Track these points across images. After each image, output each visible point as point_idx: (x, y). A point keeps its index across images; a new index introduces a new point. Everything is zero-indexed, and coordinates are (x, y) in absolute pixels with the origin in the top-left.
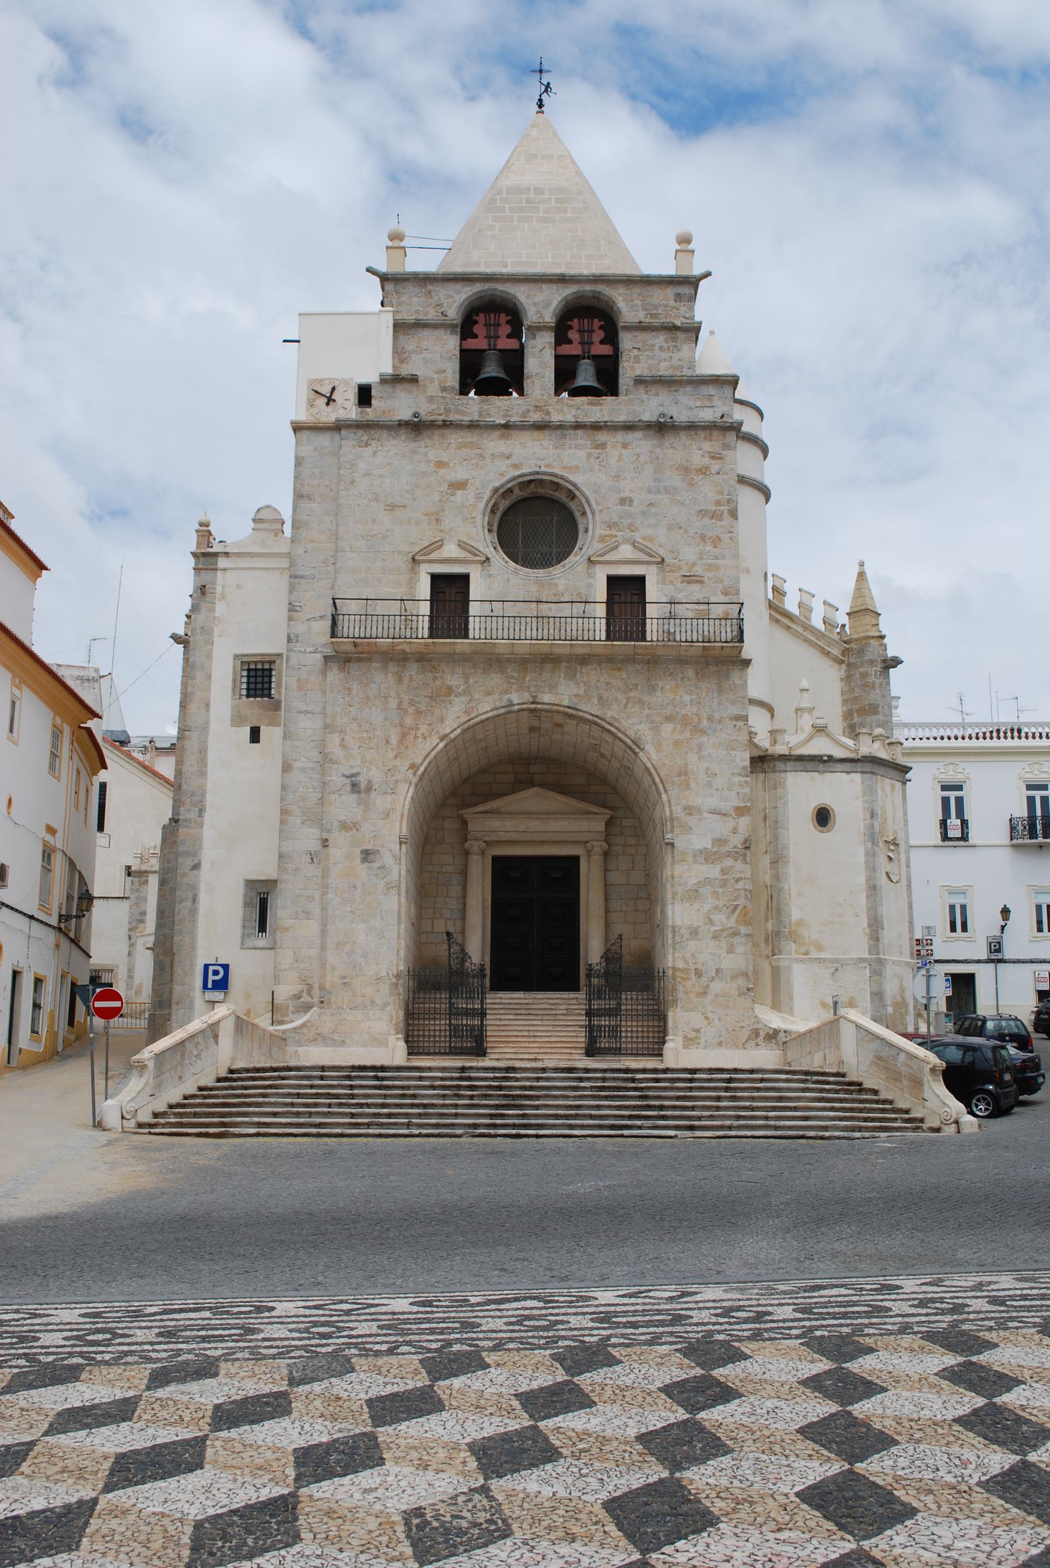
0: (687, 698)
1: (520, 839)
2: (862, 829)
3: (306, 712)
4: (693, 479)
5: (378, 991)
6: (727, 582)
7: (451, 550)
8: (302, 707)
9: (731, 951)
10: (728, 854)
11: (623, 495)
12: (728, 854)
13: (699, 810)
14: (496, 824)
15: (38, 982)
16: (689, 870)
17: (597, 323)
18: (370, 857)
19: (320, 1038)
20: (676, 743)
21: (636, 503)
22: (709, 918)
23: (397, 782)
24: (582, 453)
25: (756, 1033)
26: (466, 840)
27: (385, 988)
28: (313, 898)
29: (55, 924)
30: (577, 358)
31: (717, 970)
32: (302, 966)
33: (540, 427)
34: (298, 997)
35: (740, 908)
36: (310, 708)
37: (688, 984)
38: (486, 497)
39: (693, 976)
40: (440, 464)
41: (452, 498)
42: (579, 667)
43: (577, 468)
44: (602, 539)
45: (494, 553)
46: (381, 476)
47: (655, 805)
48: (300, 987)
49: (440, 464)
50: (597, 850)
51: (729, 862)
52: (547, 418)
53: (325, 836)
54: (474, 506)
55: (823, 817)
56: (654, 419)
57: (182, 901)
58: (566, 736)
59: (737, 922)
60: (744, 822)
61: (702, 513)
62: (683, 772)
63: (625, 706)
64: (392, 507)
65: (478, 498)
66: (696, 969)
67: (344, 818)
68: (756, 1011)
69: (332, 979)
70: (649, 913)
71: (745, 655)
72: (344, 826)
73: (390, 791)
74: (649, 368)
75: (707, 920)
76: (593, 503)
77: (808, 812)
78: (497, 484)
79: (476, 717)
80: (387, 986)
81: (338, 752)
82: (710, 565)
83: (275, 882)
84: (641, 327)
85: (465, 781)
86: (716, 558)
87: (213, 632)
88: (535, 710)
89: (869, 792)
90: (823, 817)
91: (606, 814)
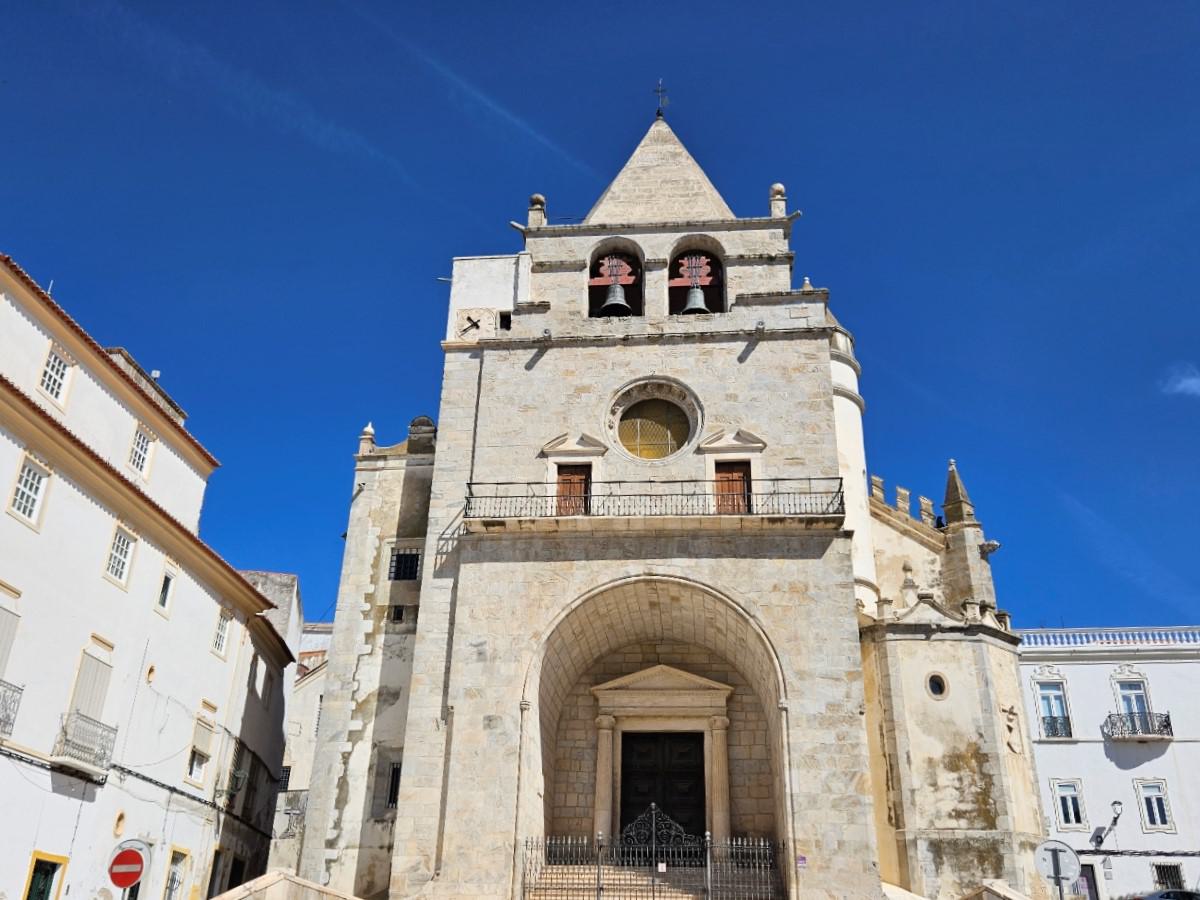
1: (646, 714)
2: (978, 697)
4: (791, 377)
5: (494, 862)
6: (828, 463)
7: (572, 444)
9: (852, 821)
10: (844, 720)
11: (728, 392)
12: (844, 720)
13: (811, 675)
14: (623, 699)
15: (177, 858)
16: (804, 735)
17: (704, 260)
18: (493, 723)
21: (740, 398)
22: (827, 786)
23: (521, 649)
24: (691, 360)
26: (597, 715)
27: (501, 858)
28: (437, 765)
29: (209, 799)
31: (841, 844)
32: (421, 835)
33: (652, 340)
34: (415, 869)
35: (859, 775)
39: (814, 848)
40: (569, 373)
41: (578, 400)
42: (690, 541)
43: (687, 370)
44: (711, 429)
45: (615, 444)
46: (516, 384)
49: (569, 373)
50: (719, 724)
51: (845, 728)
54: (597, 405)
55: (937, 685)
58: (684, 612)
59: (856, 789)
62: (794, 638)
63: (735, 576)
64: (526, 409)
65: (600, 398)
66: (817, 841)
67: (469, 685)
70: (771, 786)
71: (847, 526)
73: (513, 659)
75: (825, 788)
76: (701, 399)
78: (617, 387)
79: (596, 588)
80: (503, 858)
84: (742, 260)
85: (597, 661)
86: (816, 442)
87: (368, 522)
88: (651, 581)
89: (980, 662)
90: (937, 685)
91: (726, 690)
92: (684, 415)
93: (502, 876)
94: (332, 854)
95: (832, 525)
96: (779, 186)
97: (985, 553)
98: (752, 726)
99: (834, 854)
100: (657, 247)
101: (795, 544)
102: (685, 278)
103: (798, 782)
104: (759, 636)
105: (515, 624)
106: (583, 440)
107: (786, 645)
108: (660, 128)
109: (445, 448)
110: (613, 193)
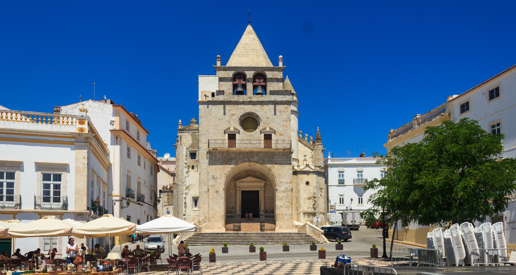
0: (280, 160)
3: (203, 163)
6: (289, 135)
7: (232, 129)
8: (203, 162)
9: (288, 210)
13: (282, 182)
19: (208, 228)
20: (278, 169)
21: (270, 118)
24: (259, 108)
25: (293, 226)
30: (258, 86)
31: (286, 214)
34: (204, 220)
36: (204, 162)
37: (280, 216)
38: (239, 117)
43: (258, 111)
44: (263, 126)
46: (217, 113)
47: (274, 181)
48: (204, 218)
51: (288, 193)
52: (251, 100)
53: (208, 188)
55: (307, 183)
56: (273, 100)
57: (179, 201)
59: (290, 204)
60: (291, 185)
61: (283, 121)
62: (279, 175)
64: (219, 119)
68: (294, 222)
69: (210, 216)
72: (212, 186)
74: (273, 88)
77: (305, 182)
78: (241, 115)
81: (210, 171)
82: (285, 132)
83: (198, 197)
86: (286, 130)
90: (307, 183)
92: (257, 121)
93: (221, 221)
94: (184, 217)
95: (289, 150)
96: (281, 56)
97: (323, 151)
98: (269, 189)
99: (285, 216)
100: (250, 74)
101: (281, 154)
102: (257, 82)
103: (278, 203)
104: (272, 174)
105: (221, 172)
106: (235, 128)
107: (278, 176)
108: (249, 28)
109: (201, 129)
110: (238, 53)
